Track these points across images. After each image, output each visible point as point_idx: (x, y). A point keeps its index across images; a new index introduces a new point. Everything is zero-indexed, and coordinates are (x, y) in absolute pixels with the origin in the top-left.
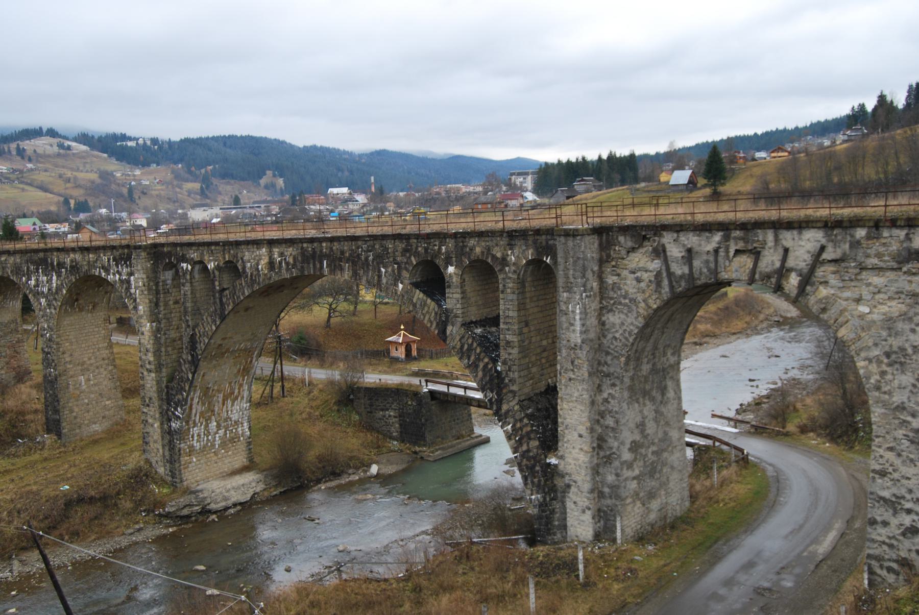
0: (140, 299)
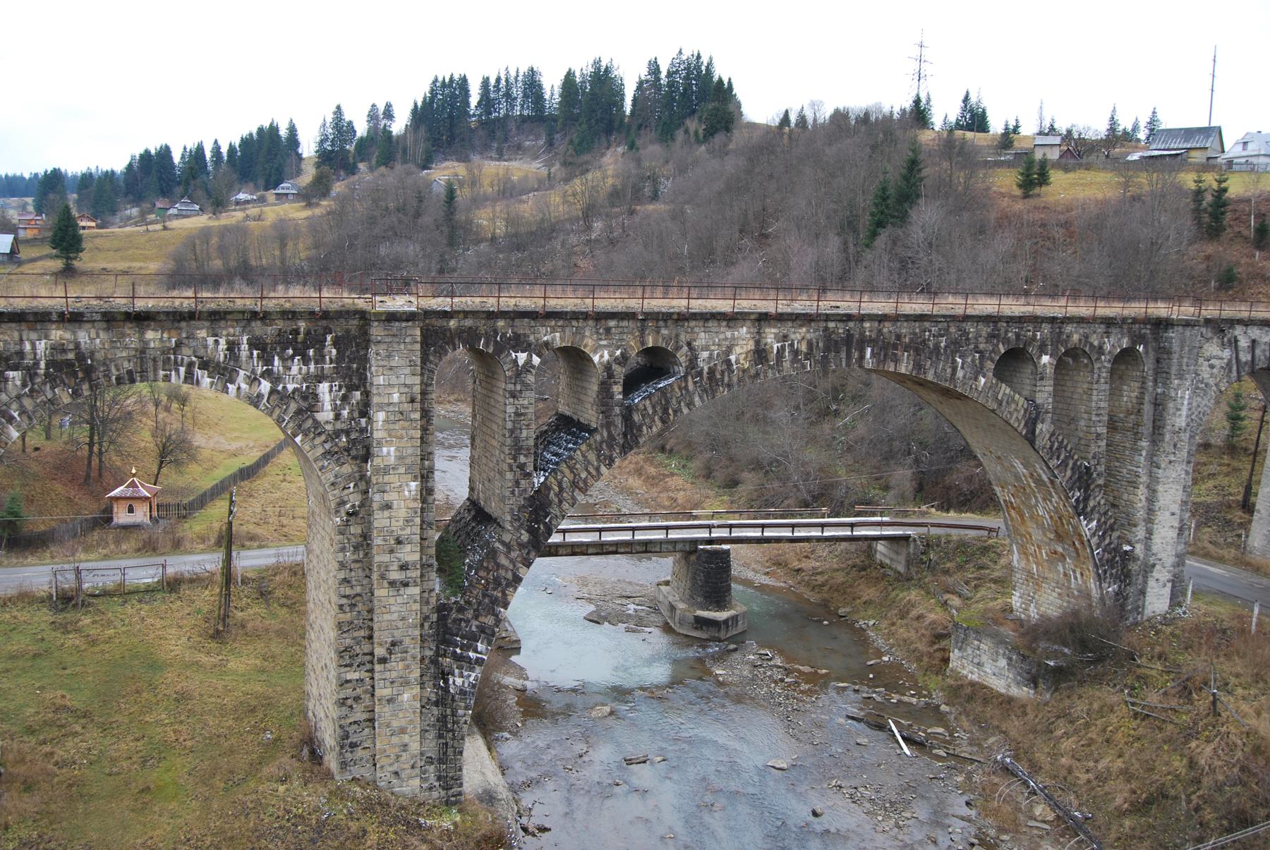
0: (389, 432)
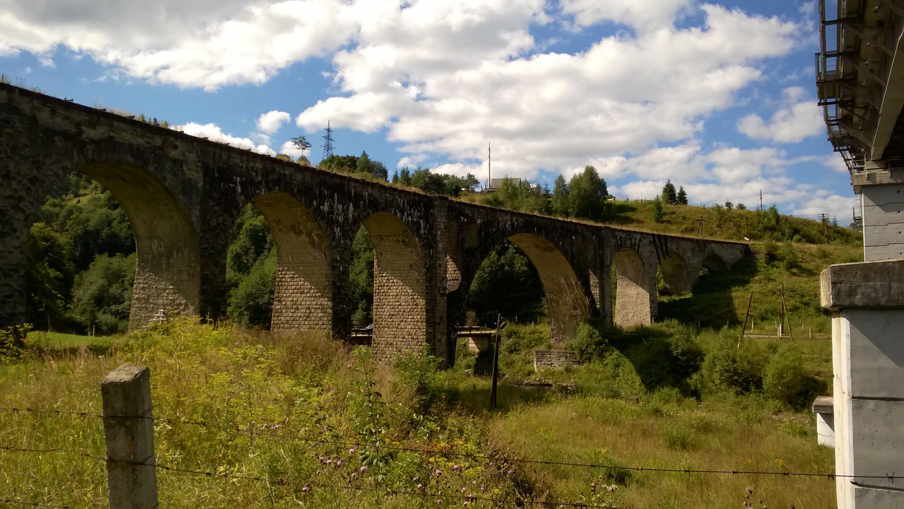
0: (441, 238)
